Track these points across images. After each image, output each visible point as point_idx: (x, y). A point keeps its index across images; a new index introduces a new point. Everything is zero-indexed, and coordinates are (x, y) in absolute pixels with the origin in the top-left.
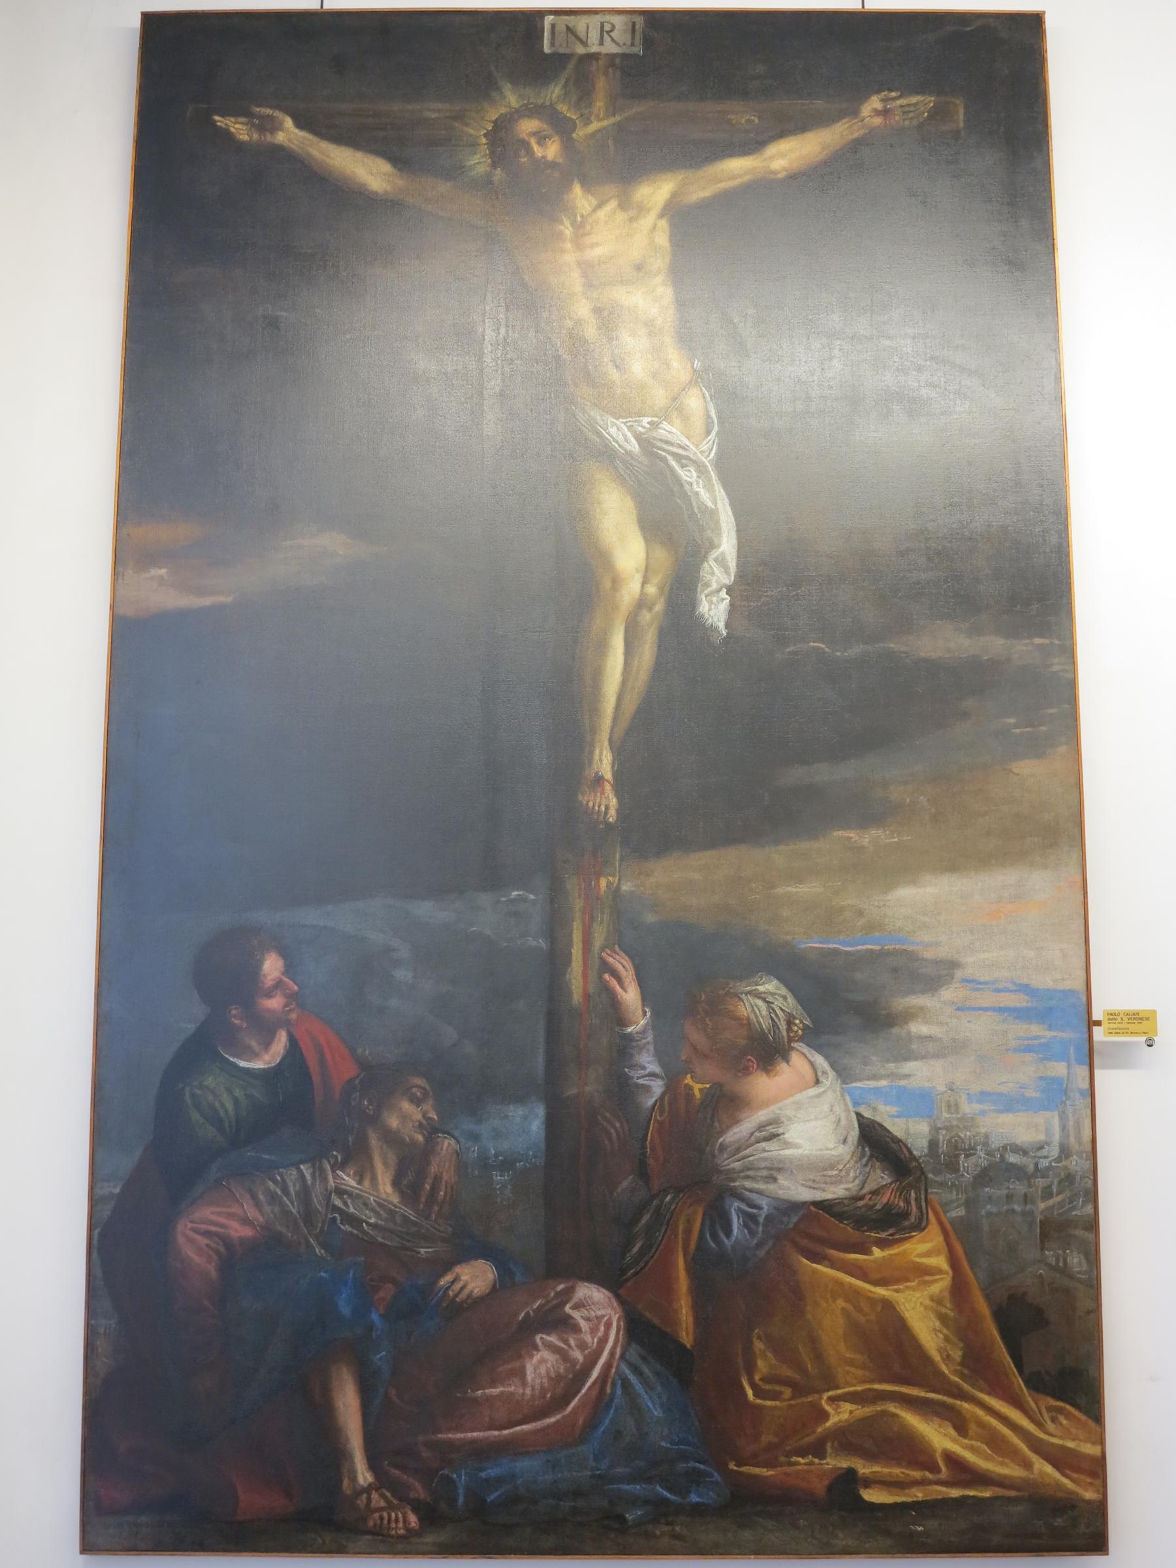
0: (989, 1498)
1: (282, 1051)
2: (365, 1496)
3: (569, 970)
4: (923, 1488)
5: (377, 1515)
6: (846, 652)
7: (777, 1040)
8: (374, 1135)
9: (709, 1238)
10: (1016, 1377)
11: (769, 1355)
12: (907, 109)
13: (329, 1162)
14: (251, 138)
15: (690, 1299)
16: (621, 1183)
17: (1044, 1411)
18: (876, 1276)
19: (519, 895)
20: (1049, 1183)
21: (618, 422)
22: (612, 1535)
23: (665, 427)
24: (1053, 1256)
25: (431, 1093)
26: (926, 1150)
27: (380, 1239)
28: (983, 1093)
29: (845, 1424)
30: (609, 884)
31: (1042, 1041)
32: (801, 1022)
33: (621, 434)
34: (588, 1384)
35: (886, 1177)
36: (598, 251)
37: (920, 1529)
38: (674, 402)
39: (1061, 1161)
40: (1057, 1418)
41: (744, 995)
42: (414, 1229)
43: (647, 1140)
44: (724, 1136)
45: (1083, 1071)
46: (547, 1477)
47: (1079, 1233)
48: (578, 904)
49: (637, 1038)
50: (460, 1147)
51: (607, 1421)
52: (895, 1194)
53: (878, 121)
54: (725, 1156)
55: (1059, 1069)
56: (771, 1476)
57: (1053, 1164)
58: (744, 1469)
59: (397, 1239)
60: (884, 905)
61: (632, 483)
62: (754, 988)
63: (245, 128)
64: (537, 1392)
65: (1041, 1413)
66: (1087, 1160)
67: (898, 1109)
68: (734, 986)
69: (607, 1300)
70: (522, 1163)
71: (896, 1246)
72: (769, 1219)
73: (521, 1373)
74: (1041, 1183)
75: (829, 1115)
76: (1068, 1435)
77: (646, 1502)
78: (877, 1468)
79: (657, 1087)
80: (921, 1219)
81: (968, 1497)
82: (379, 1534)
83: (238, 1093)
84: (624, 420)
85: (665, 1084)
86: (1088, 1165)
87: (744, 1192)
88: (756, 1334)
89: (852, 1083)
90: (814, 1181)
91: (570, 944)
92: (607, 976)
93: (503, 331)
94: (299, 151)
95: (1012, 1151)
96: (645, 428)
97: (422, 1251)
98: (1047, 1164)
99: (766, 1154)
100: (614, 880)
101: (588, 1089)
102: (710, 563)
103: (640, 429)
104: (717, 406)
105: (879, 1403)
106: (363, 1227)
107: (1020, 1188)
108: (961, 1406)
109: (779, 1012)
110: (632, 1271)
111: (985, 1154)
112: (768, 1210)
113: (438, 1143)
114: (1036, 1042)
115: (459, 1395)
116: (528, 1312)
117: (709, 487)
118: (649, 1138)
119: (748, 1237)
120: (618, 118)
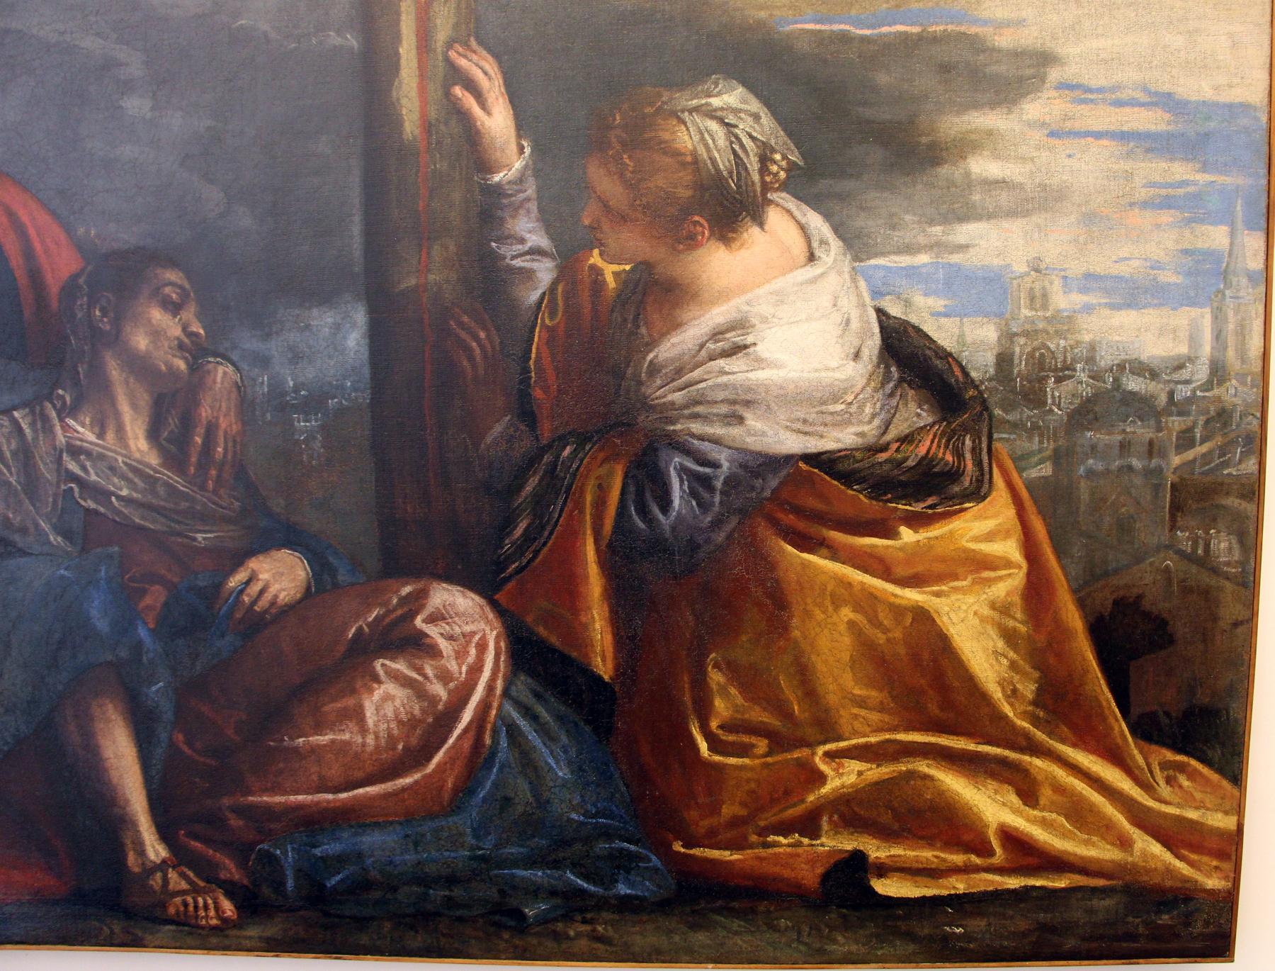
0: (1063, 888)
2: (159, 875)
3: (396, 83)
5: (178, 900)
7: (744, 188)
8: (114, 363)
10: (1117, 720)
11: (733, 691)
13: (54, 406)
15: (606, 608)
16: (491, 428)
18: (900, 571)
20: (1190, 424)
22: (506, 936)
24: (1188, 538)
26: (992, 371)
27: (137, 520)
28: (1089, 276)
29: (850, 790)
31: (1191, 189)
32: (784, 157)
34: (457, 733)
35: (924, 414)
37: (959, 930)
39: (1212, 389)
40: (1175, 778)
42: (184, 505)
44: (656, 350)
46: (407, 857)
47: (1232, 502)
49: (510, 192)
50: (241, 378)
51: (488, 784)
52: (940, 441)
54: (659, 382)
55: (1217, 237)
57: (1198, 393)
58: (697, 851)
59: (163, 520)
62: (703, 102)
64: (383, 742)
65: (1151, 772)
66: (1252, 387)
67: (946, 302)
68: (671, 99)
69: (478, 610)
70: (336, 400)
71: (938, 525)
72: (732, 482)
73: (357, 715)
74: (1176, 423)
75: (830, 314)
76: (1189, 800)
77: (553, 893)
78: (897, 851)
79: (545, 272)
80: (980, 481)
81: (1034, 887)
82: (184, 925)
85: (557, 266)
86: (1253, 395)
87: (690, 439)
88: (711, 660)
90: (805, 421)
91: (397, 39)
92: (458, 91)
97: (199, 536)
99: (725, 379)
101: (431, 277)
106: (111, 502)
107: (1141, 431)
111: (1090, 377)
112: (729, 469)
113: (209, 372)
114: (1181, 191)
115: (272, 744)
118: (533, 356)
119: (698, 513)
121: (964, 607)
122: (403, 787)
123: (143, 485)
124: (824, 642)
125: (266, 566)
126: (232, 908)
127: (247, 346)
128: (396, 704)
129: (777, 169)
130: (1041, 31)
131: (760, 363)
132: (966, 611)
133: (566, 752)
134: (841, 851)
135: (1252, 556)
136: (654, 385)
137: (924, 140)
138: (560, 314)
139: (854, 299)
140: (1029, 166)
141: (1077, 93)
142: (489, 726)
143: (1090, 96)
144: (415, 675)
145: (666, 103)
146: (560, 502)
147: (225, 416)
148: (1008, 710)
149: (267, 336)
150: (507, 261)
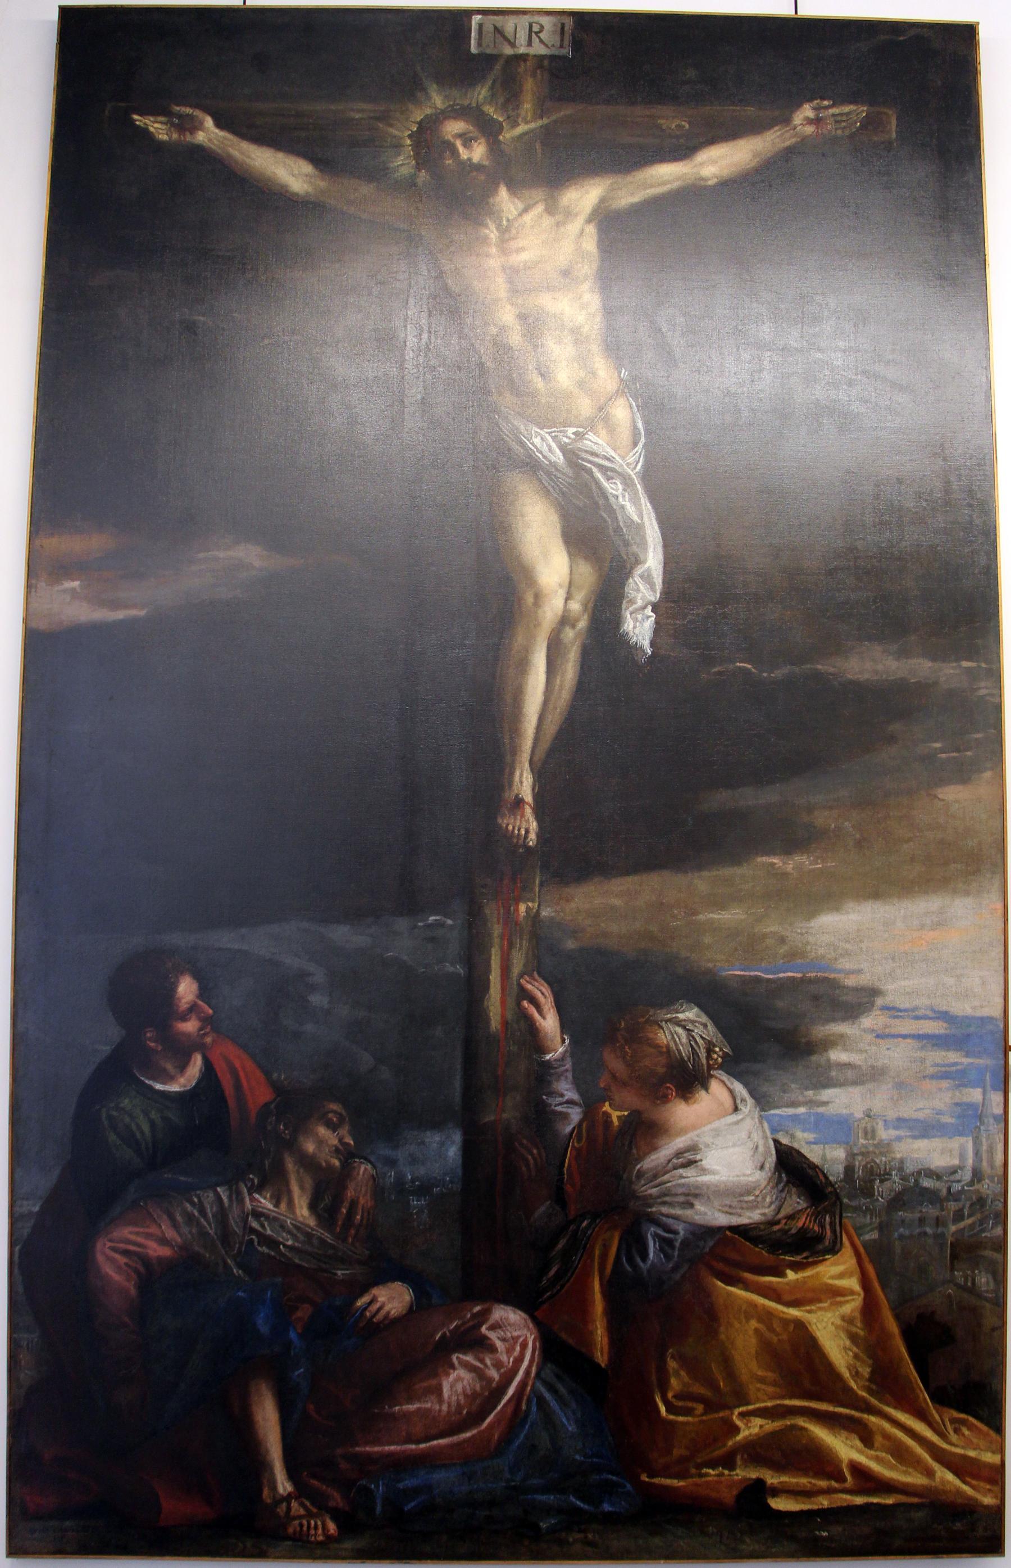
1: (197, 1075)
2: (284, 1504)
4: (828, 1496)
5: (297, 1522)
6: (773, 673)
7: (697, 1067)
9: (625, 1261)
10: (921, 1391)
11: (683, 1373)
12: (839, 118)
13: (246, 1186)
14: (170, 138)
15: (605, 1321)
17: (948, 1424)
18: (787, 1297)
19: (436, 920)
21: (541, 432)
22: (526, 1543)
23: (590, 438)
24: (961, 1276)
25: (347, 1119)
26: (842, 1176)
27: (297, 1261)
28: (899, 1119)
29: (755, 1438)
30: (528, 909)
31: (959, 1067)
32: (721, 1050)
33: (545, 445)
34: (503, 1402)
35: (801, 1202)
36: (524, 256)
37: (825, 1534)
38: (600, 412)
40: (960, 1430)
41: (664, 1023)
42: (330, 1252)
43: (564, 1166)
44: (642, 1163)
45: (997, 1098)
47: (988, 1253)
48: (497, 930)
51: (522, 1436)
53: (810, 129)
55: (975, 1095)
56: (681, 1486)
57: (966, 1188)
58: (656, 1480)
60: (807, 933)
61: (556, 495)
62: (674, 1016)
63: (164, 127)
64: (453, 1409)
65: (944, 1426)
66: (998, 1183)
67: (815, 1136)
68: (654, 1015)
69: (523, 1321)
71: (809, 1270)
72: (685, 1243)
73: (438, 1391)
74: (953, 1207)
76: (969, 1444)
78: (784, 1478)
79: (575, 1115)
80: (835, 1242)
81: (872, 1504)
83: (153, 1115)
84: (549, 430)
86: (999, 1188)
89: (770, 1110)
90: (730, 1206)
92: (525, 1003)
93: (425, 336)
94: (219, 151)
95: (925, 1176)
96: (570, 438)
97: (339, 1273)
98: (960, 1188)
99: (683, 1181)
100: (534, 905)
101: (505, 1116)
102: (636, 579)
103: (566, 440)
104: (643, 417)
105: (788, 1417)
106: (280, 1249)
108: (868, 1420)
109: (698, 1039)
110: (548, 1294)
111: (902, 1179)
112: (684, 1235)
113: (354, 1168)
114: (954, 1068)
115: (376, 1411)
116: (445, 1333)
117: (635, 501)
118: (566, 1165)
120: (546, 121)
121: (825, 1320)
122: (464, 1439)
123: (303, 1238)
124: (739, 1342)
125: (383, 1293)
126: (335, 1527)
127: (382, 1152)
128: (464, 1383)
129: (717, 1057)
130: (872, 976)
131: (704, 1171)
132: (826, 1322)
133: (574, 1413)
134: (750, 1479)
135: (1002, 1287)
136: (640, 1184)
137: (803, 1040)
138: (584, 1139)
139: (760, 1133)
140: (864, 1055)
141: (892, 1013)
142: (525, 1398)
143: (900, 1014)
144: (478, 1364)
145: (651, 1016)
146: (579, 1255)
147: (363, 1196)
148: (853, 1384)
149: (396, 1147)
150: (553, 1107)
